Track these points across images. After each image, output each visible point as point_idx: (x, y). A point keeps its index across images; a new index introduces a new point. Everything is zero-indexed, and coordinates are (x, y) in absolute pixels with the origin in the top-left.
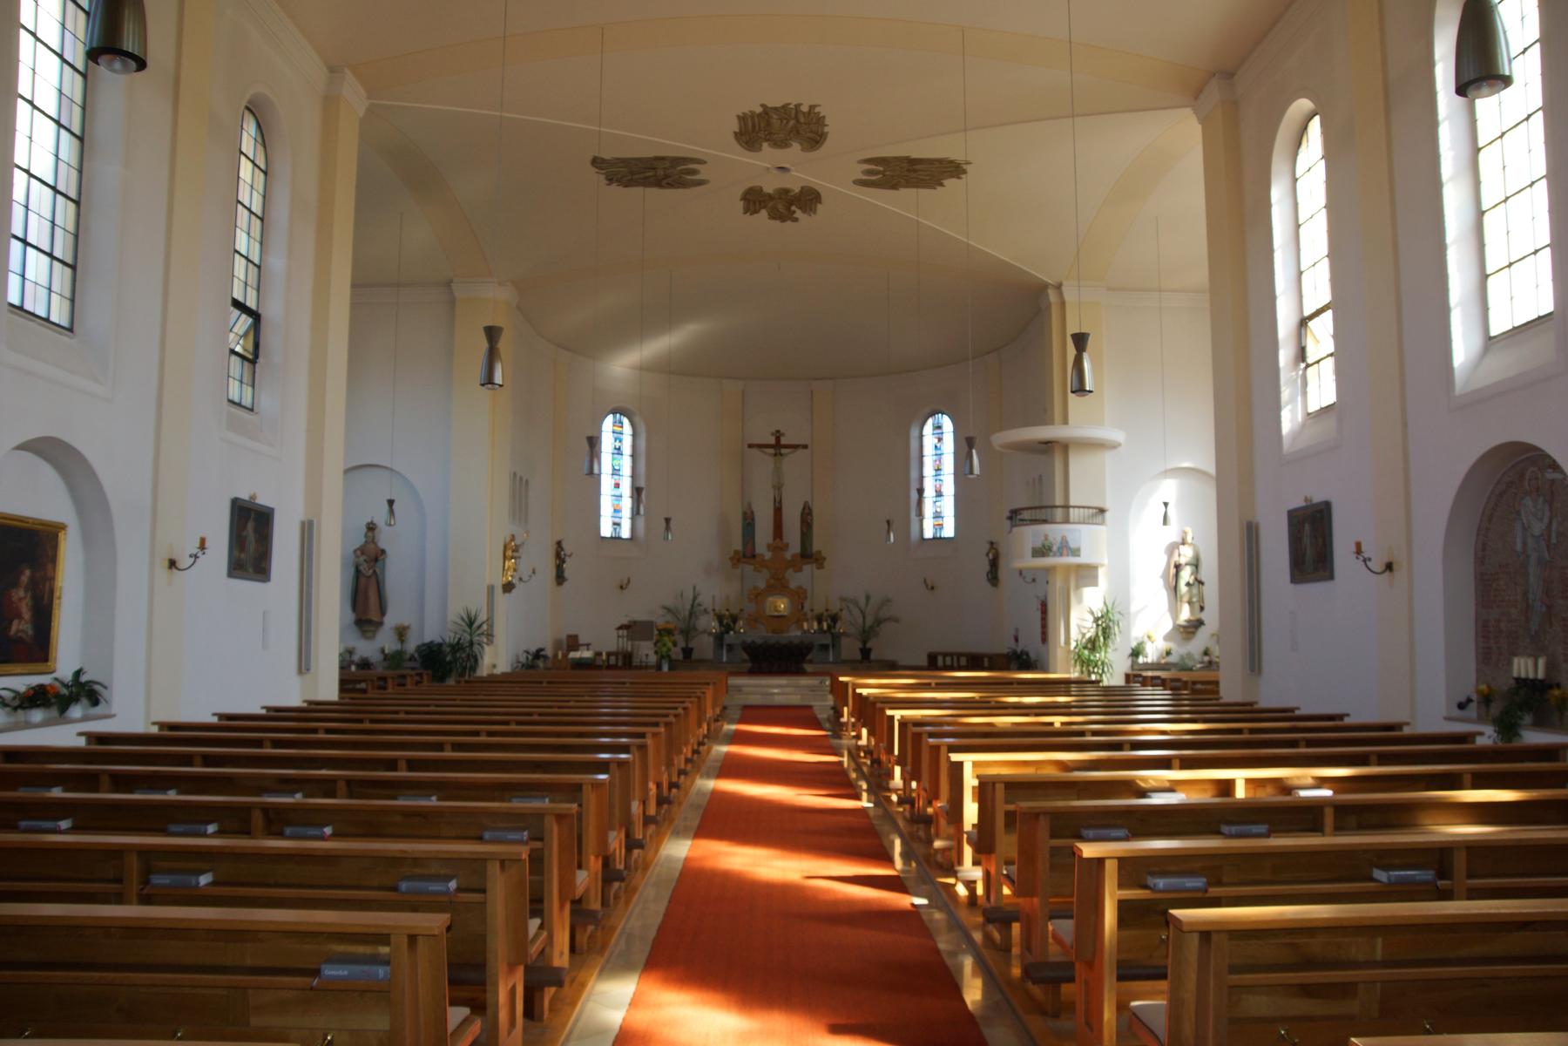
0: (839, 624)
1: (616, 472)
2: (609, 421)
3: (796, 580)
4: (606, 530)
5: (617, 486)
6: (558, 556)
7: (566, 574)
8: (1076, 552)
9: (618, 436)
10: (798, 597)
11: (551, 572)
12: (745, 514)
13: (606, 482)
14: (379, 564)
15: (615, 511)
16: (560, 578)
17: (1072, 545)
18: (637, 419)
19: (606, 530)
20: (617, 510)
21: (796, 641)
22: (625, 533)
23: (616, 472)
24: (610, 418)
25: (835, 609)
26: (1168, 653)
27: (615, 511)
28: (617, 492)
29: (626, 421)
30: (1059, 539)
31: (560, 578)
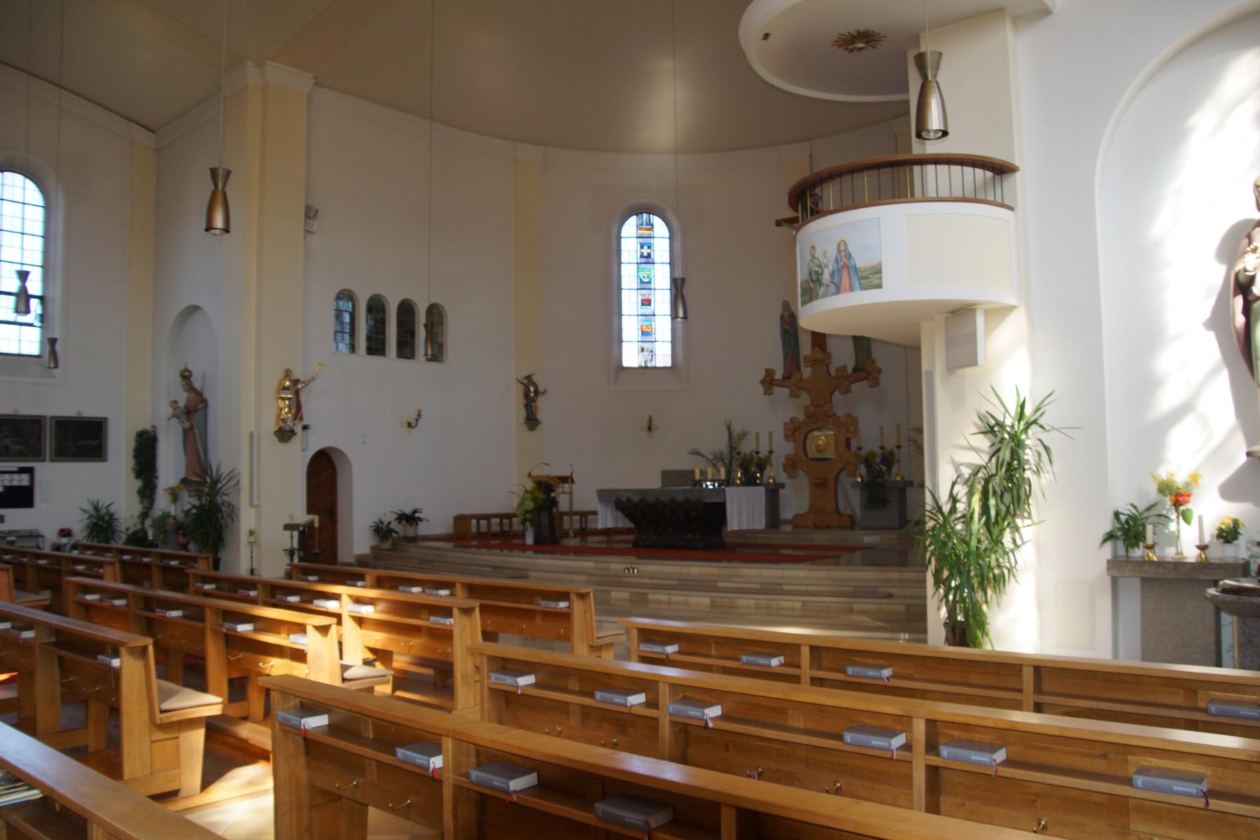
0: (895, 469)
1: (645, 285)
2: (630, 227)
3: (840, 404)
4: (631, 357)
5: (646, 302)
6: (527, 395)
7: (539, 416)
8: (871, 278)
9: (645, 241)
10: (847, 428)
11: (517, 412)
12: (782, 317)
13: (630, 301)
14: (199, 415)
15: (647, 333)
16: (532, 421)
17: (862, 260)
18: (670, 216)
19: (631, 357)
20: (646, 333)
21: (680, 498)
22: (663, 358)
23: (645, 285)
24: (633, 220)
25: (890, 445)
26: (1229, 535)
27: (647, 333)
28: (647, 310)
29: (657, 221)
30: (833, 253)
31: (532, 421)
